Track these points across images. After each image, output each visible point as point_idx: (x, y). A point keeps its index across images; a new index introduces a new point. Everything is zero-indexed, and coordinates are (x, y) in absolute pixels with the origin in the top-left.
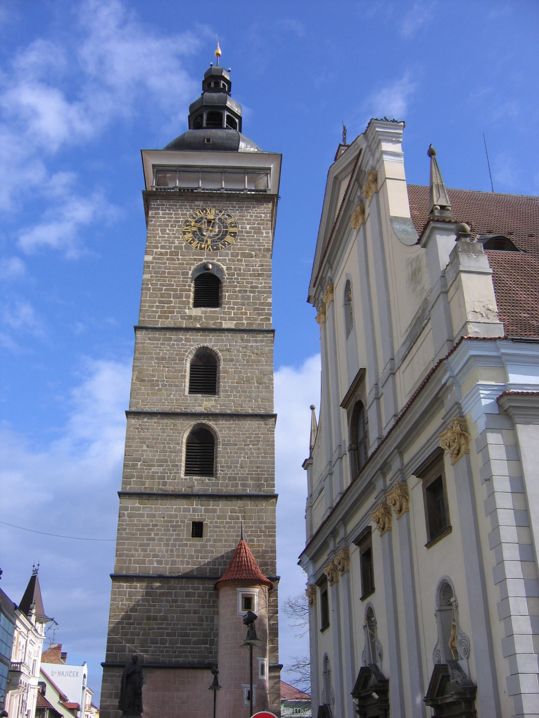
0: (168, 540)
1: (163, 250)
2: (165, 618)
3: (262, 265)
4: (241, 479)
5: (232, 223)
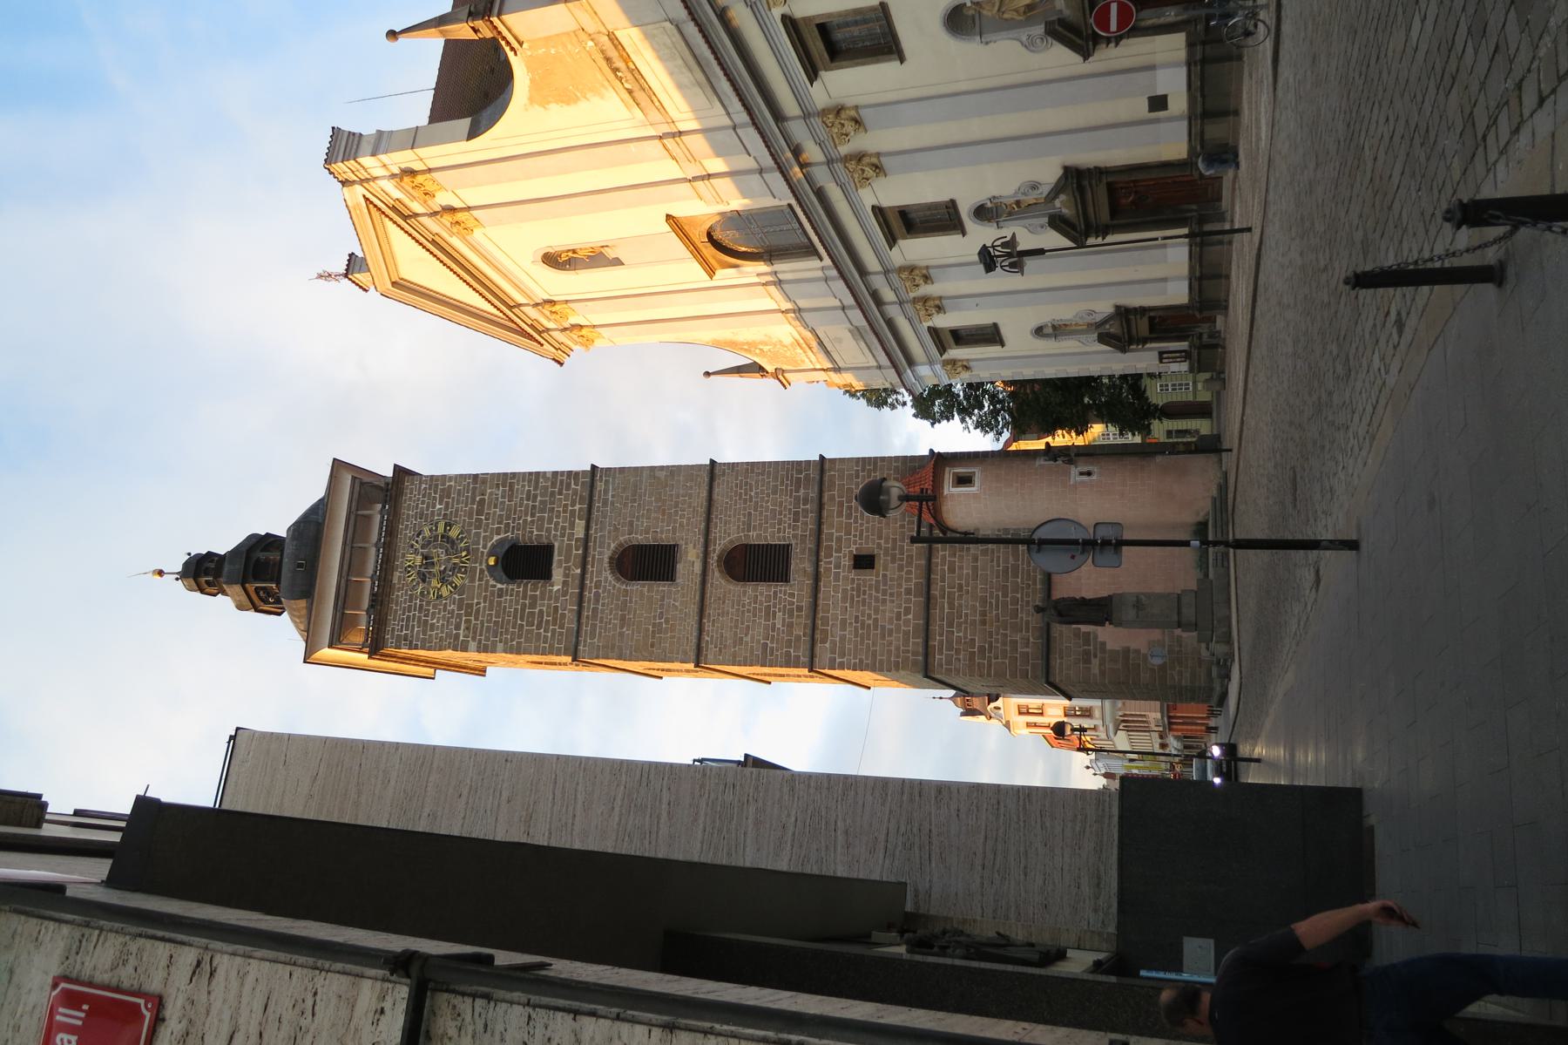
0: (877, 600)
2: (984, 601)
4: (797, 505)
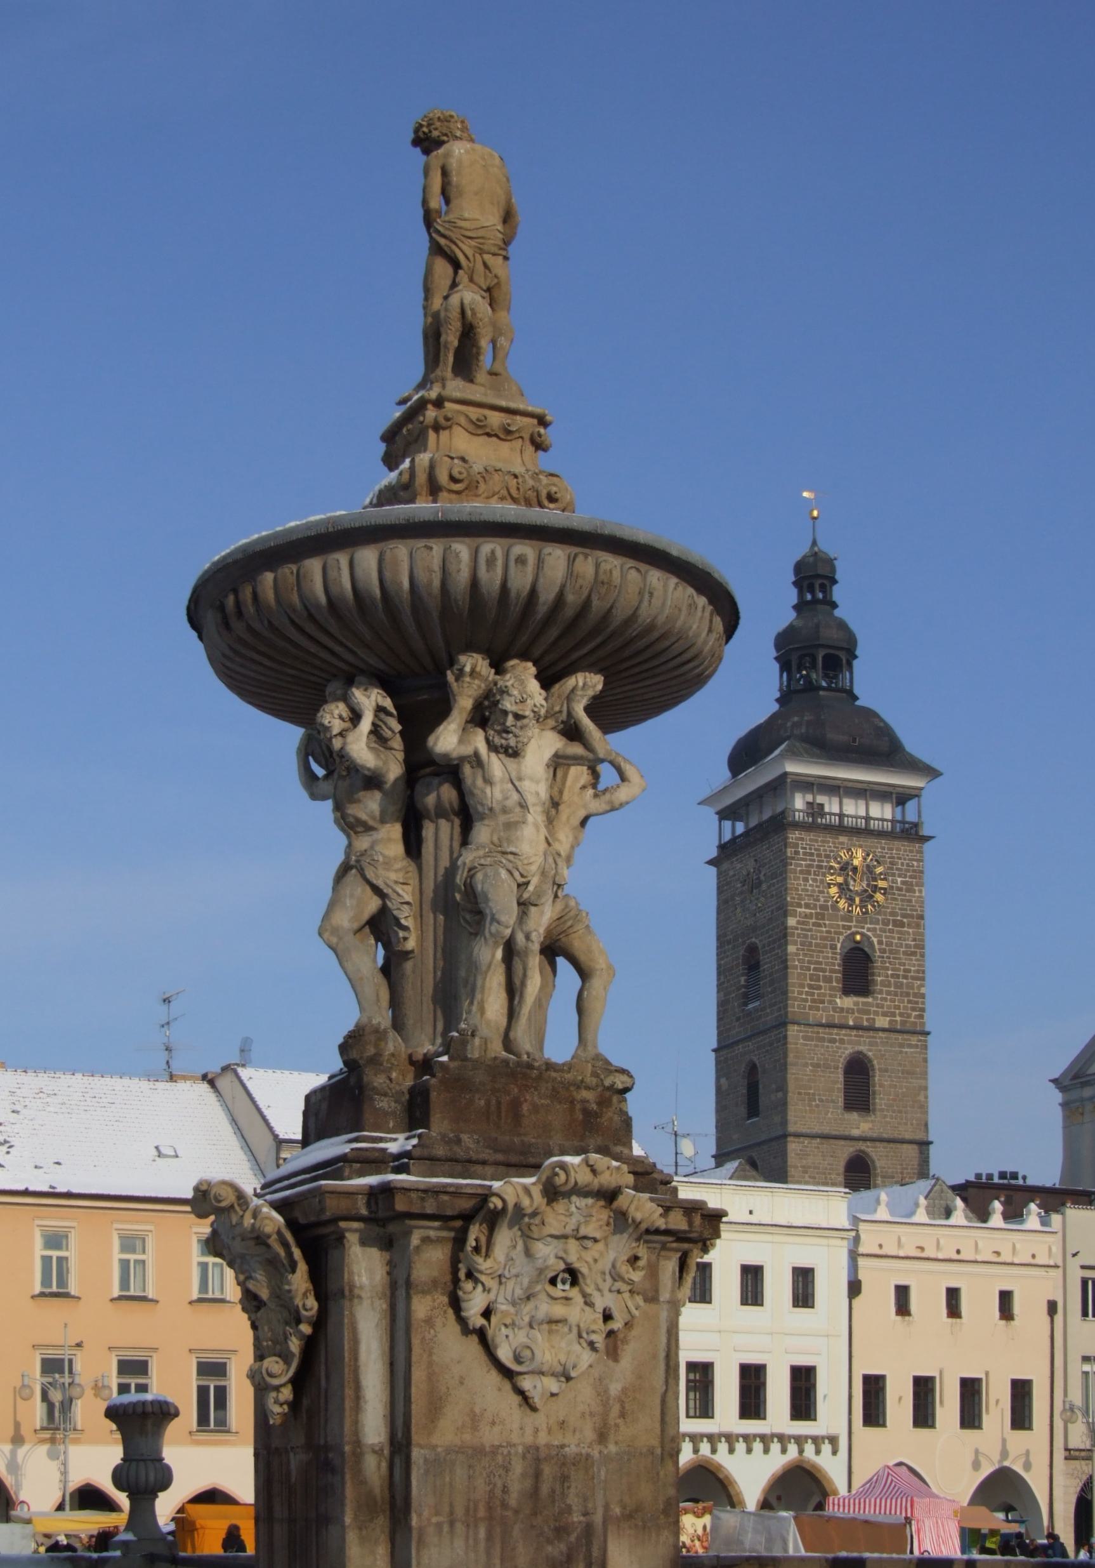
1: (808, 911)
3: (914, 940)
5: (881, 874)
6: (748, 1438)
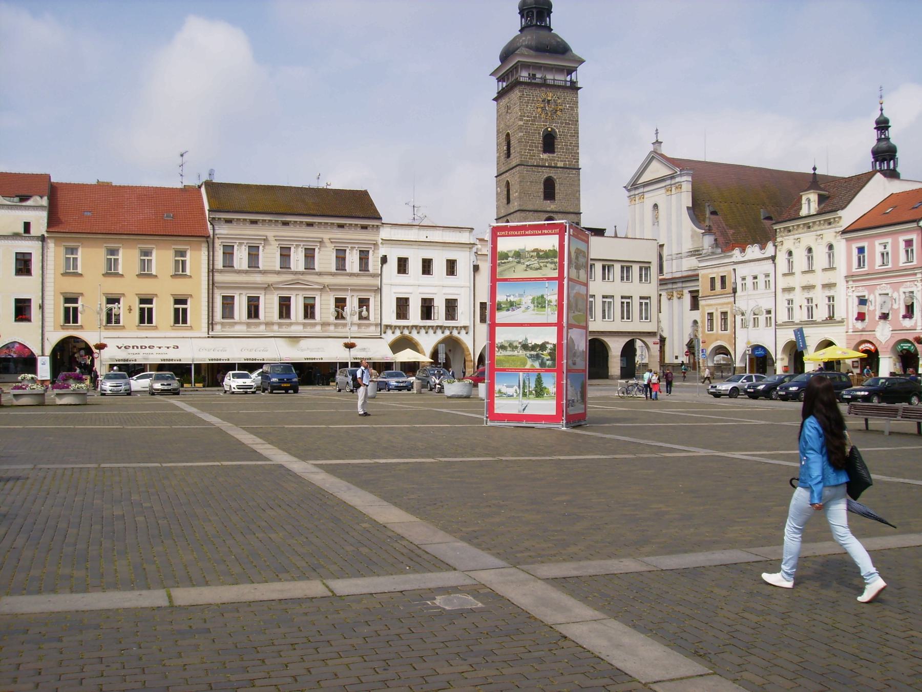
6: (424, 327)
